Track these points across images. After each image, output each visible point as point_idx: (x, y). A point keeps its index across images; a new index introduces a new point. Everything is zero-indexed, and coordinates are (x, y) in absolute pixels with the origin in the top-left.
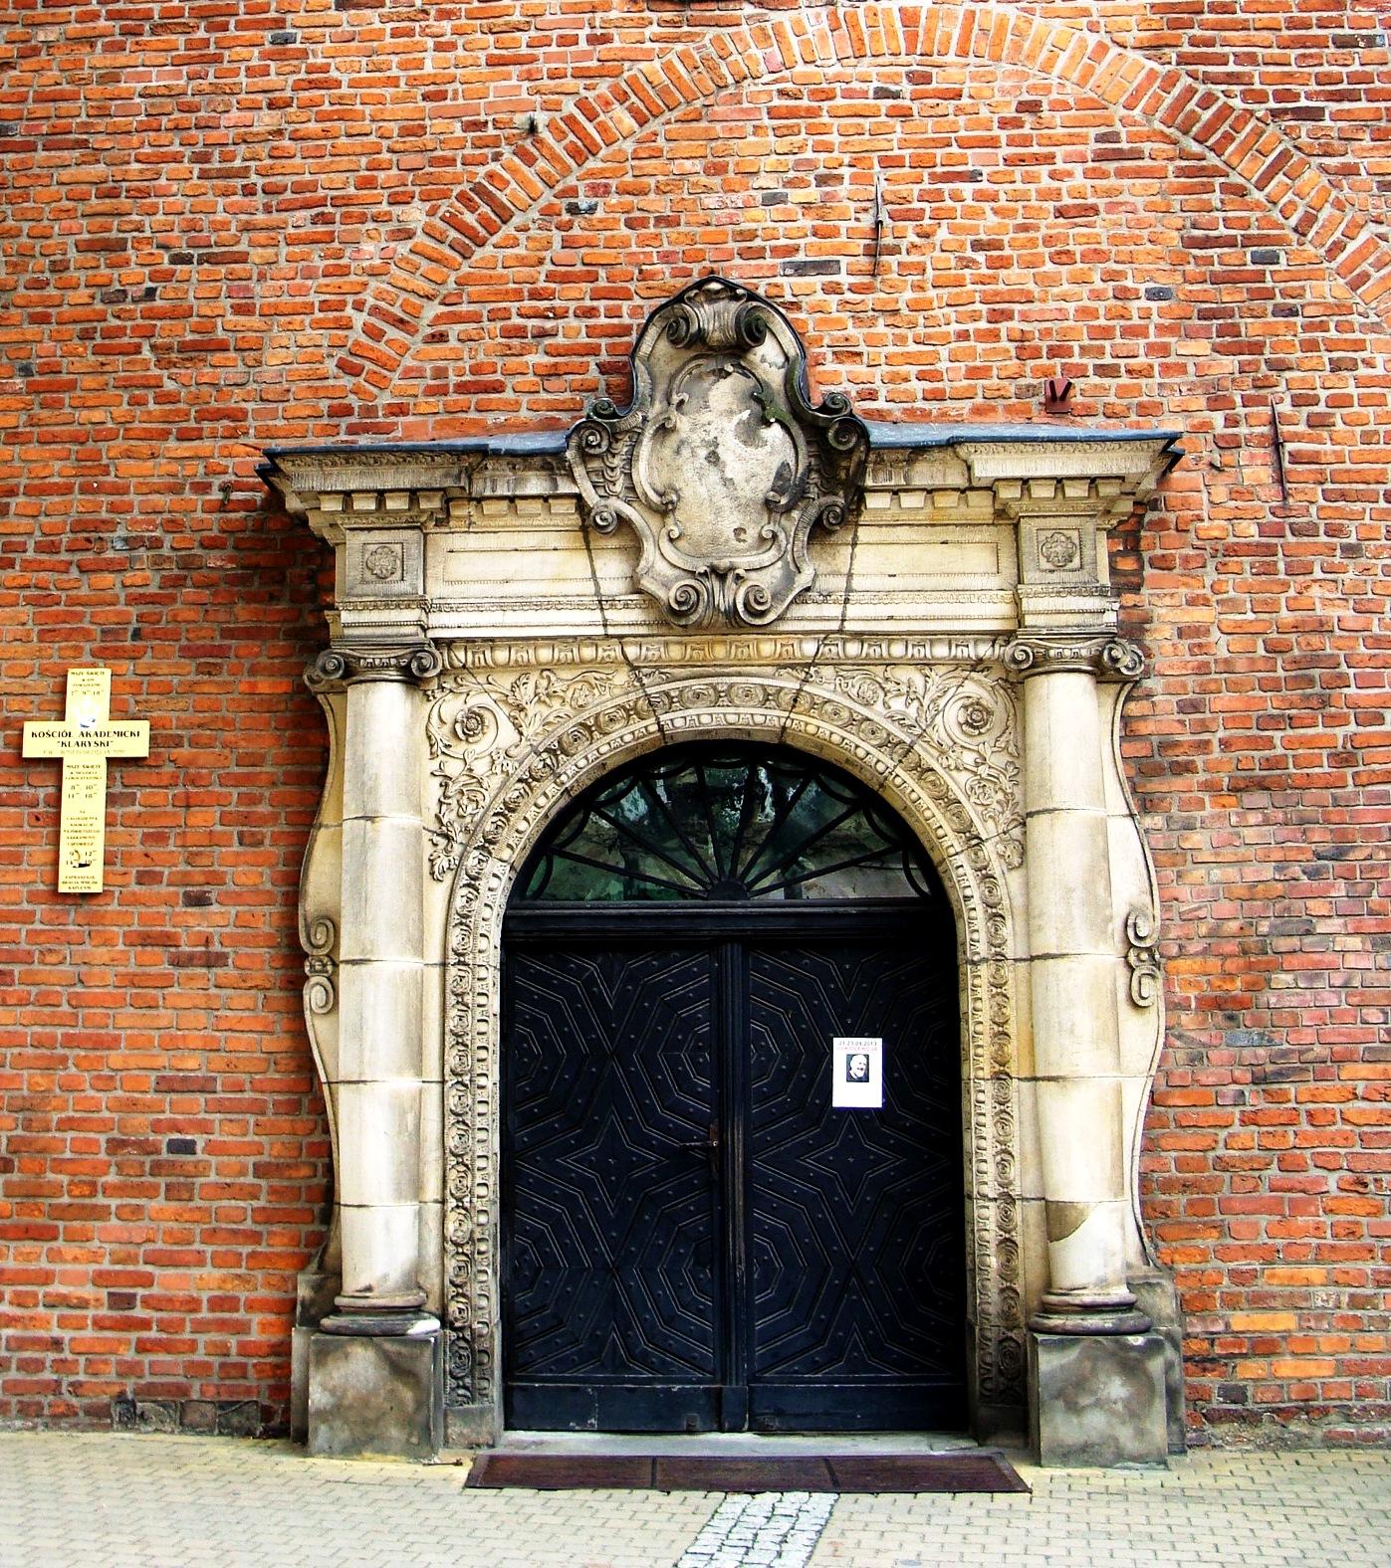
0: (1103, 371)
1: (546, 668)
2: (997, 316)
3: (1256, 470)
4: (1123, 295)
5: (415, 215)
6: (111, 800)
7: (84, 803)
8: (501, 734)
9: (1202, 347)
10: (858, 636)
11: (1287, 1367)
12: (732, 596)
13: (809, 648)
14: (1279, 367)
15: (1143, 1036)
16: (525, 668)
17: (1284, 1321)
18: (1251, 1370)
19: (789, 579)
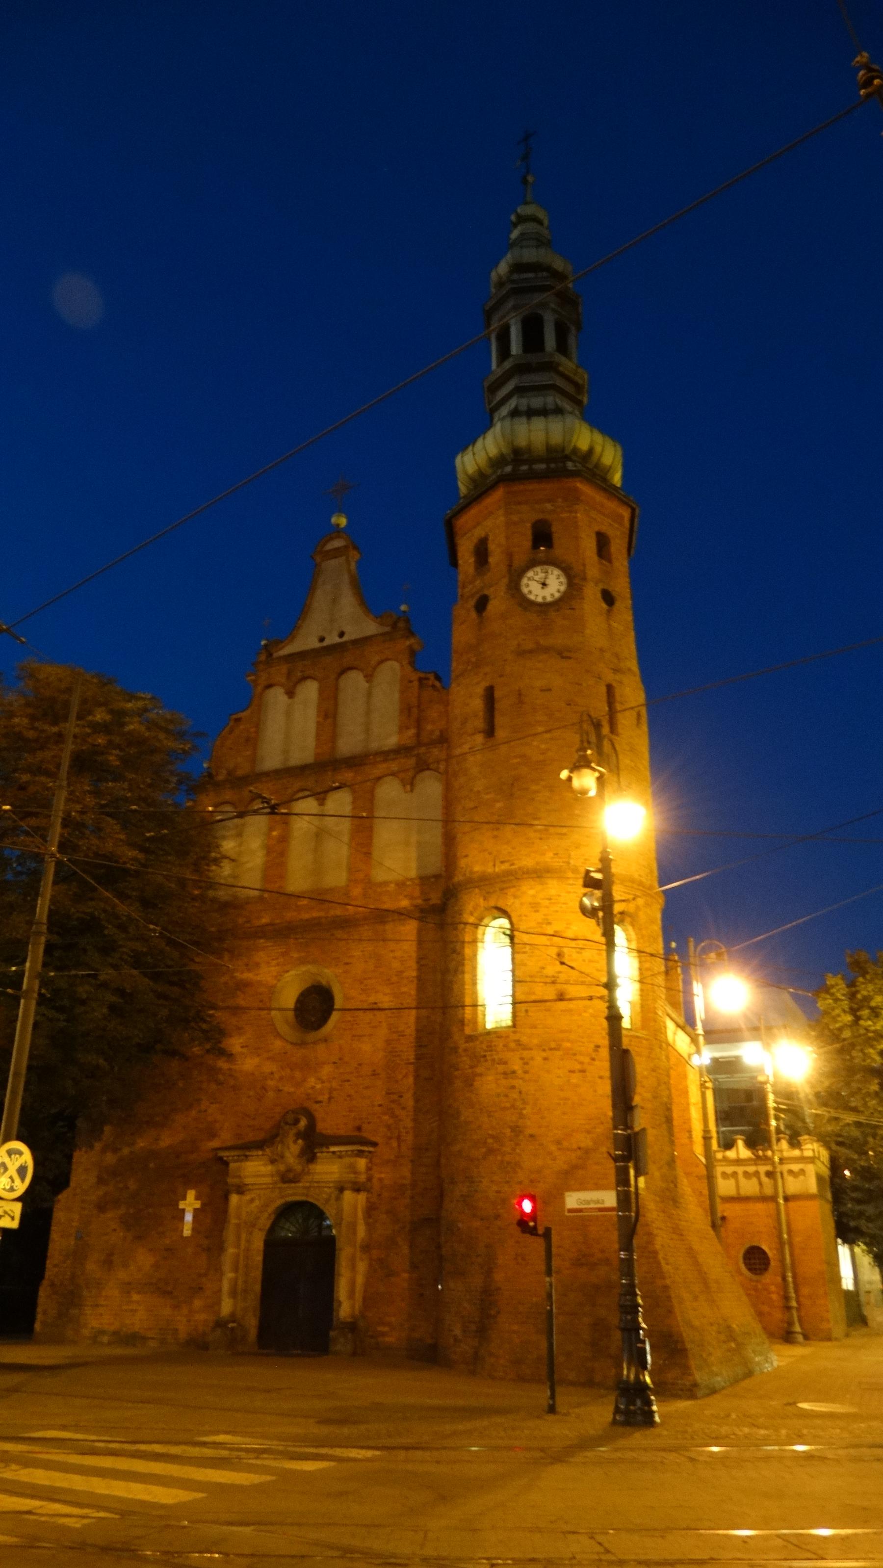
0: (369, 1123)
1: (265, 1189)
2: (351, 1111)
3: (395, 1144)
4: (373, 1106)
5: (251, 1093)
6: (194, 1217)
7: (189, 1217)
8: (257, 1203)
9: (386, 1118)
10: (318, 1182)
11: (387, 1339)
12: (291, 1175)
13: (308, 1184)
14: (400, 1120)
15: (362, 1267)
16: (259, 1189)
17: (386, 1329)
18: (381, 1339)
19: (303, 1170)
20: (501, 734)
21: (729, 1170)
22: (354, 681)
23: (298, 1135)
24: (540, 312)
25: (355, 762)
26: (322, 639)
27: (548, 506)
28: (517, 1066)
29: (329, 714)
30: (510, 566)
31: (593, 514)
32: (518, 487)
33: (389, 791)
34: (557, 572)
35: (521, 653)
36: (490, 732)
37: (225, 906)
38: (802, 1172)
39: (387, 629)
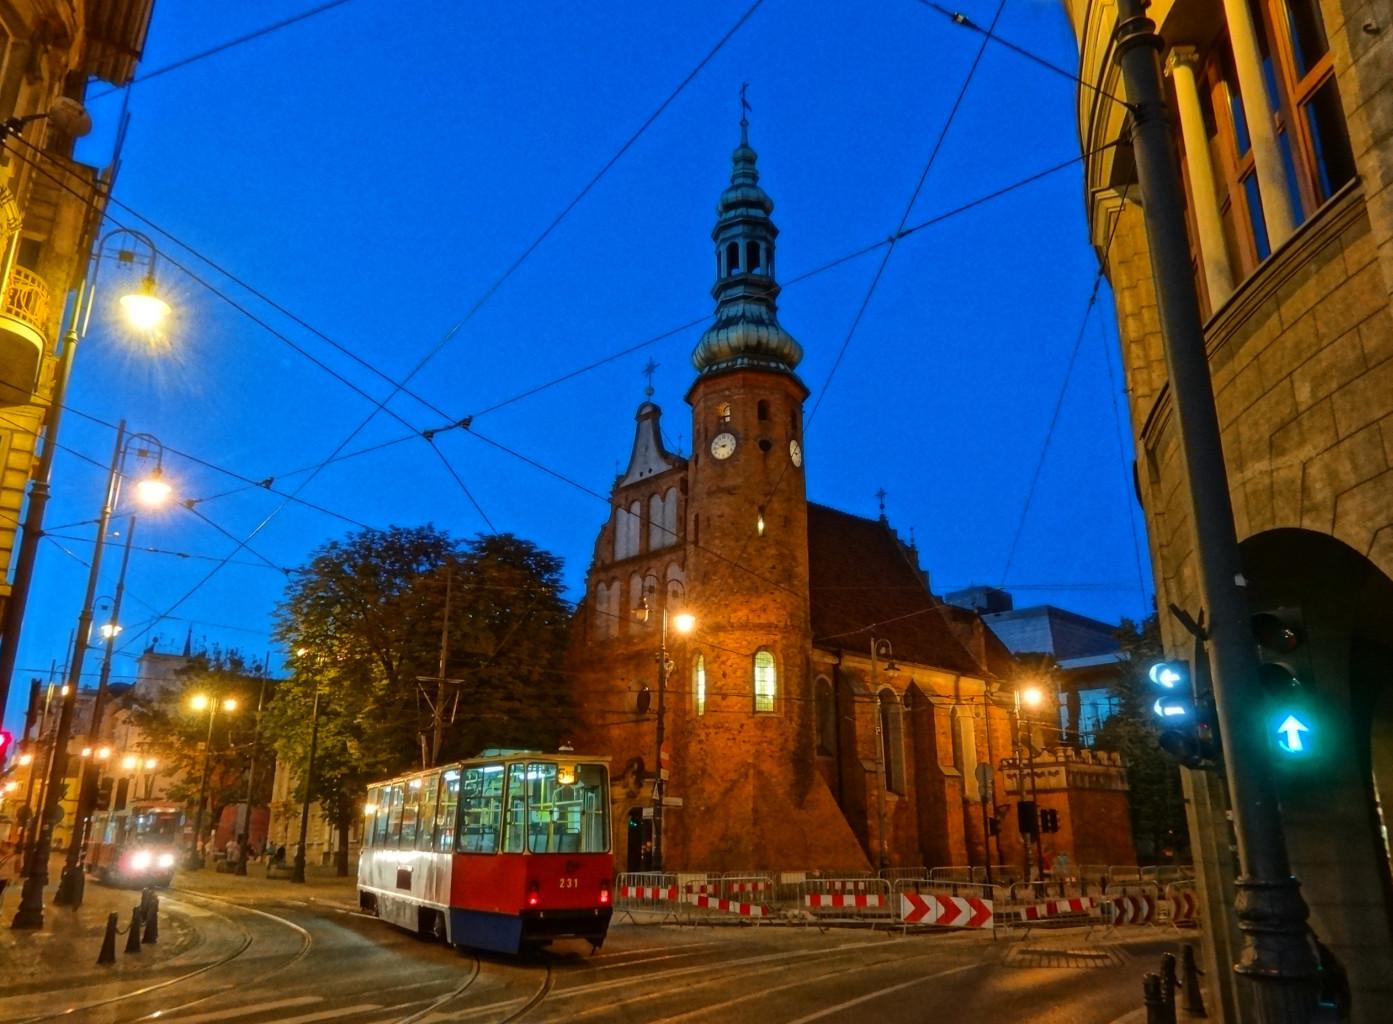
20: (701, 544)
21: (1012, 772)
22: (656, 501)
23: (634, 773)
24: (737, 241)
25: (658, 554)
26: (641, 474)
27: (727, 393)
28: (703, 737)
29: (646, 522)
30: (706, 436)
31: (756, 391)
32: (709, 383)
33: (674, 572)
34: (731, 437)
35: (710, 494)
36: (696, 543)
37: (605, 644)
38: (1057, 773)
39: (670, 467)
